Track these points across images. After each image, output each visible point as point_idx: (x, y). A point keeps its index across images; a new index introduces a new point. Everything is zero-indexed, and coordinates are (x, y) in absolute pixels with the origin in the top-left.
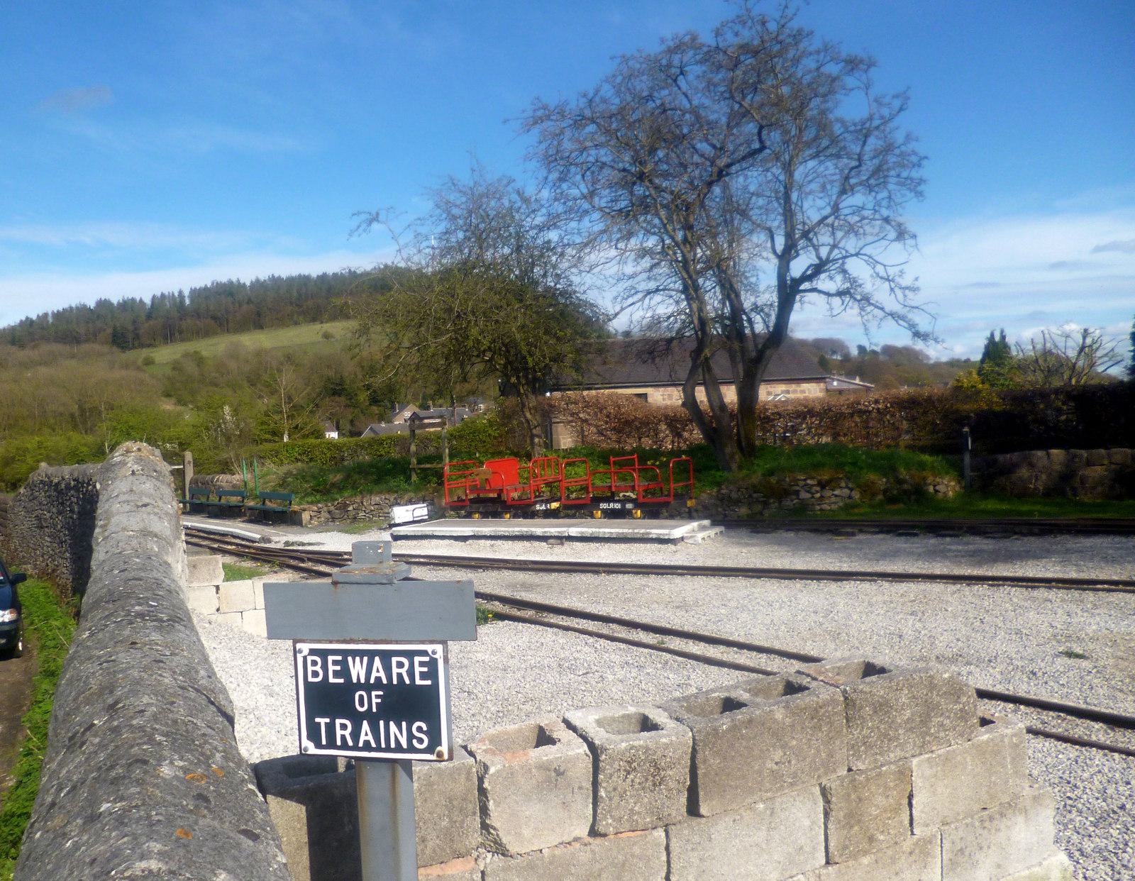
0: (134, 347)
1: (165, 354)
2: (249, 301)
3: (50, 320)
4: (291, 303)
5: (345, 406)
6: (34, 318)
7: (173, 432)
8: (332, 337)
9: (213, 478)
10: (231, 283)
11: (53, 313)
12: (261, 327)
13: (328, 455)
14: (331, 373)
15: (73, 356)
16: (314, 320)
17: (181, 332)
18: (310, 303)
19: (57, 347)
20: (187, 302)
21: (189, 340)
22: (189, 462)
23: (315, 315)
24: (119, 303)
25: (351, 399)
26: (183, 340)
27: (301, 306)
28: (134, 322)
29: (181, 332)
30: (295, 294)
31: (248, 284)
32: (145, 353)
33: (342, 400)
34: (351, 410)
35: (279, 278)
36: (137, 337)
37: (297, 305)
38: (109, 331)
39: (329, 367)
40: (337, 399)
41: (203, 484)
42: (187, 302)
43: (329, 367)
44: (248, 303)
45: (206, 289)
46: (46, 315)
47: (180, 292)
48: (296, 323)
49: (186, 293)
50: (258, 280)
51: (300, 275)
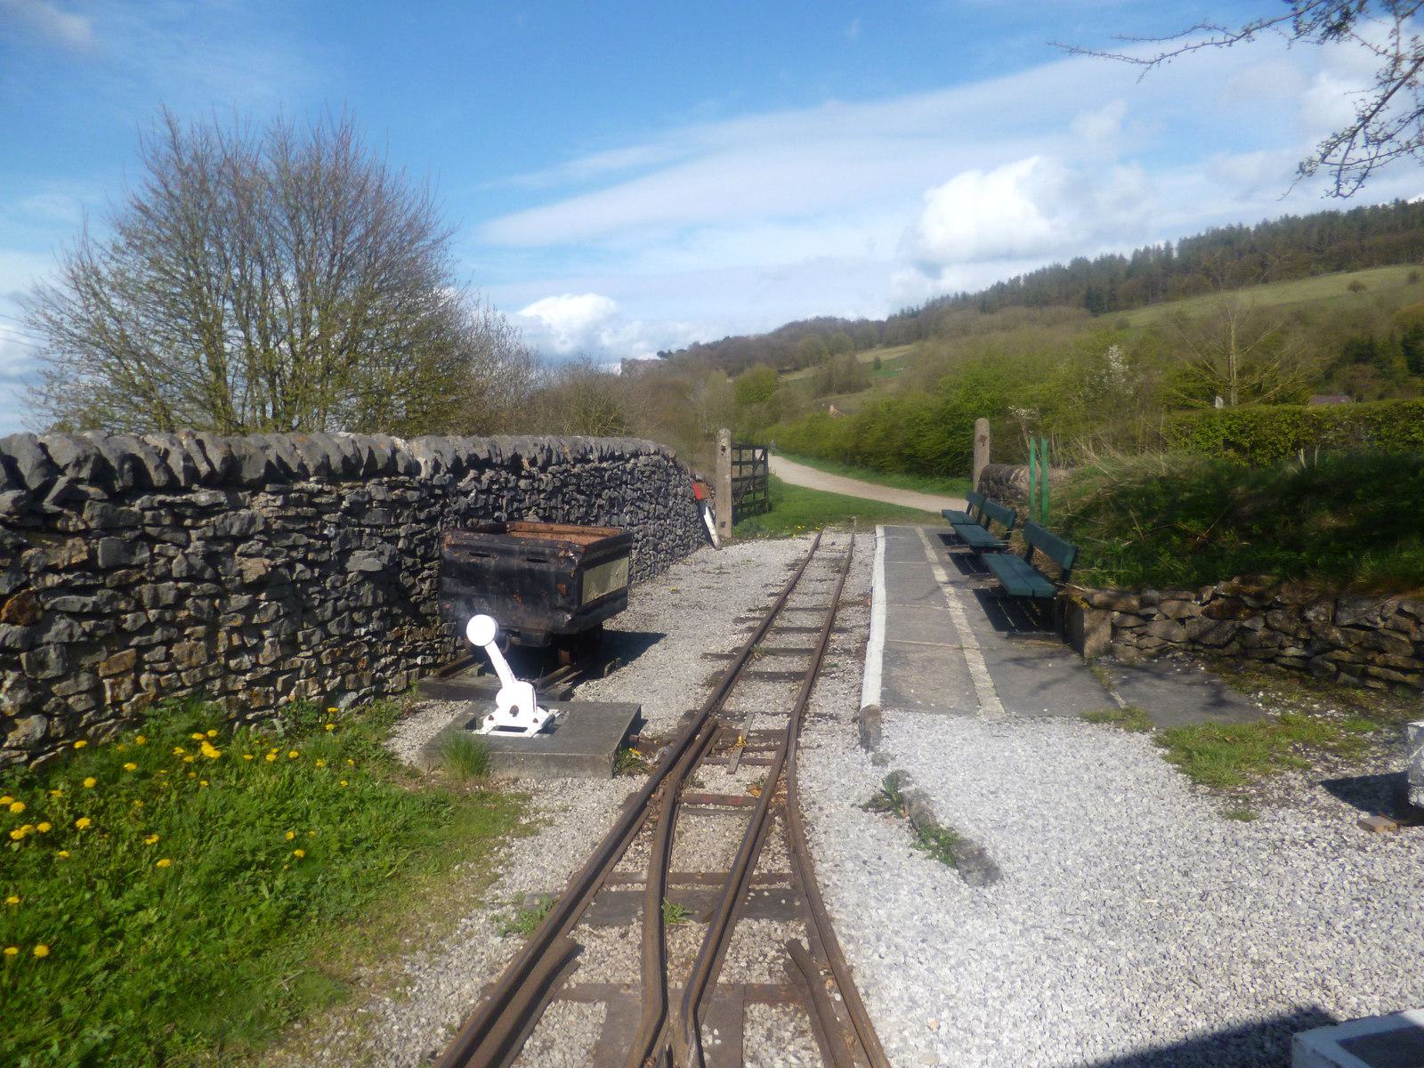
0: (1110, 310)
1: (1142, 317)
2: (1253, 250)
3: (1022, 282)
4: (1309, 249)
5: (1373, 377)
6: (1006, 282)
7: (1034, 389)
8: (1364, 288)
9: (1011, 472)
10: (1231, 228)
11: (1025, 276)
12: (1266, 281)
13: (1291, 436)
14: (1357, 334)
15: (1033, 321)
16: (1339, 268)
17: (1164, 291)
18: (1335, 248)
19: (1022, 311)
20: (1175, 254)
21: (1174, 300)
22: (983, 439)
23: (1341, 263)
24: (1096, 262)
25: (1381, 368)
26: (1168, 300)
27: (1322, 252)
28: (1111, 281)
29: (1164, 291)
30: (1315, 237)
31: (1252, 229)
32: (1121, 315)
33: (1369, 369)
34: (1381, 381)
35: (1295, 219)
36: (1113, 298)
37: (1317, 251)
38: (1083, 292)
39: (1354, 326)
40: (1362, 367)
41: (996, 483)
42: (1175, 254)
43: (1354, 326)
44: (1250, 252)
45: (1199, 238)
46: (1018, 278)
47: (1168, 245)
48: (1313, 274)
49: (1175, 244)
50: (1266, 223)
51: (1324, 213)
